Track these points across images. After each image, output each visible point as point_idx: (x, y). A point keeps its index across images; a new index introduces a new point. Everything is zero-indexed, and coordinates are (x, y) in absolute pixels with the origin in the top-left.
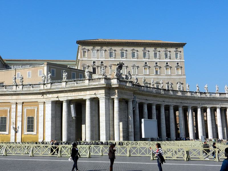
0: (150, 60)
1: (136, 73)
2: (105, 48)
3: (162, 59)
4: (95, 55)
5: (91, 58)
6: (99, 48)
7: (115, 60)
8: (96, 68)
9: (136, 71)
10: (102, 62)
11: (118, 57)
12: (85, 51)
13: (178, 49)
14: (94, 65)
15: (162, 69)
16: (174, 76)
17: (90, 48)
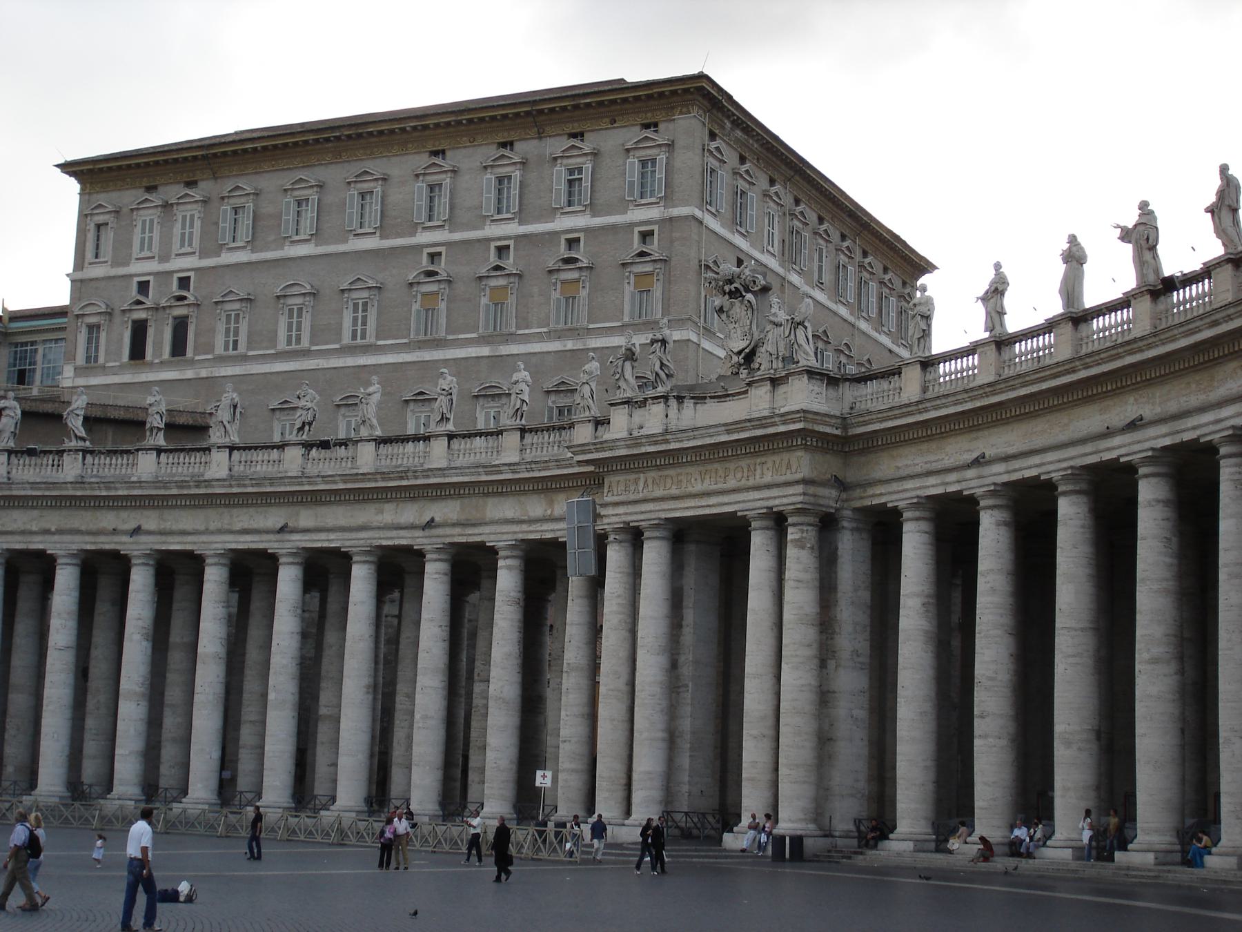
0: (457, 236)
1: (363, 337)
2: (207, 186)
3: (539, 219)
4: (151, 239)
5: (127, 264)
6: (173, 192)
7: (255, 257)
8: (146, 321)
9: (364, 323)
10: (184, 282)
11: (272, 238)
12: (101, 219)
13: (662, 127)
14: (139, 303)
15: (535, 290)
16: (610, 331)
17: (129, 197)
